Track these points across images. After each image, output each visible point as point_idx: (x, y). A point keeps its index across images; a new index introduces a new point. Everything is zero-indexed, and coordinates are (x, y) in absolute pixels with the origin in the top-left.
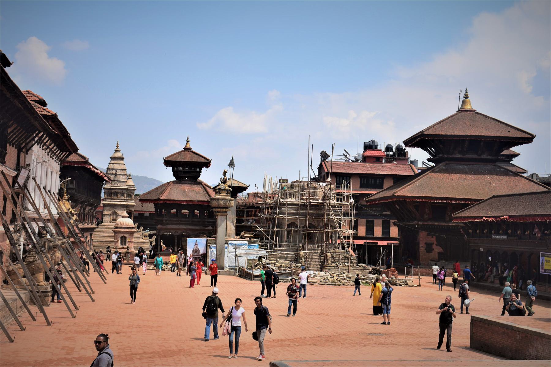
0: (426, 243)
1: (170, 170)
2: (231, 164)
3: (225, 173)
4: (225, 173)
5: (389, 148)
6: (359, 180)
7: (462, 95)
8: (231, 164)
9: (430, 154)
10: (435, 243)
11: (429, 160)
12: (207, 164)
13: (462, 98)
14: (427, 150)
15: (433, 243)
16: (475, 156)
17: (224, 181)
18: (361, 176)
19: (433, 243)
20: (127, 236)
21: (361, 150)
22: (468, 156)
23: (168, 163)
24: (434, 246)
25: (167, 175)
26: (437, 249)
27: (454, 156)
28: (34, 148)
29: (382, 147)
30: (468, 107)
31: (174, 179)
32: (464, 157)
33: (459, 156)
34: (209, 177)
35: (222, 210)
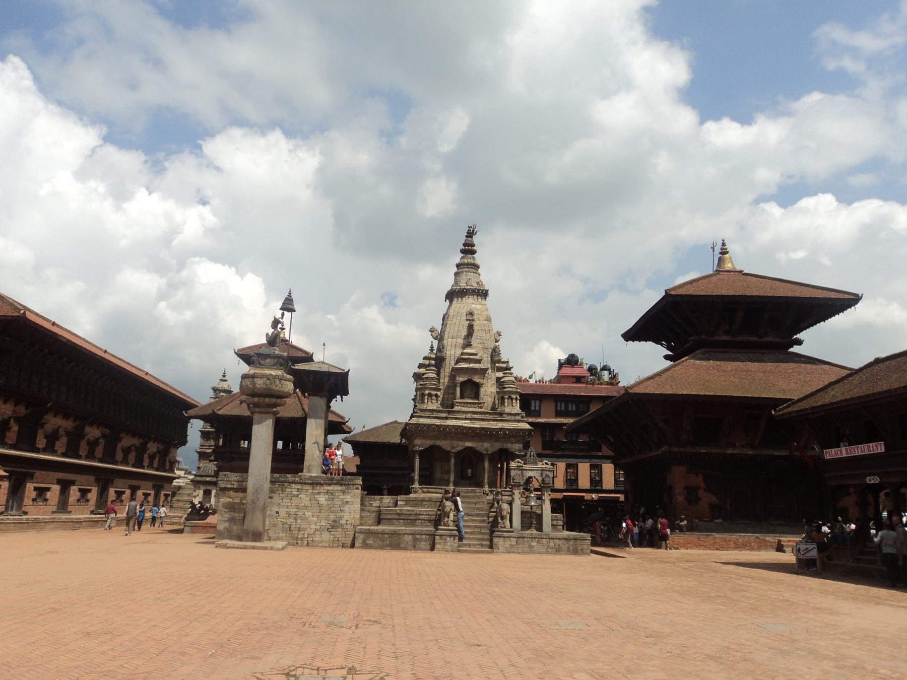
0: (686, 488)
4: (276, 323)
6: (553, 405)
7: (718, 249)
9: (669, 348)
10: (703, 486)
11: (667, 357)
15: (699, 488)
16: (755, 339)
17: (273, 340)
18: (557, 398)
19: (699, 488)
22: (739, 338)
24: (701, 493)
26: (707, 499)
27: (717, 338)
30: (728, 266)
32: (735, 339)
35: (261, 400)
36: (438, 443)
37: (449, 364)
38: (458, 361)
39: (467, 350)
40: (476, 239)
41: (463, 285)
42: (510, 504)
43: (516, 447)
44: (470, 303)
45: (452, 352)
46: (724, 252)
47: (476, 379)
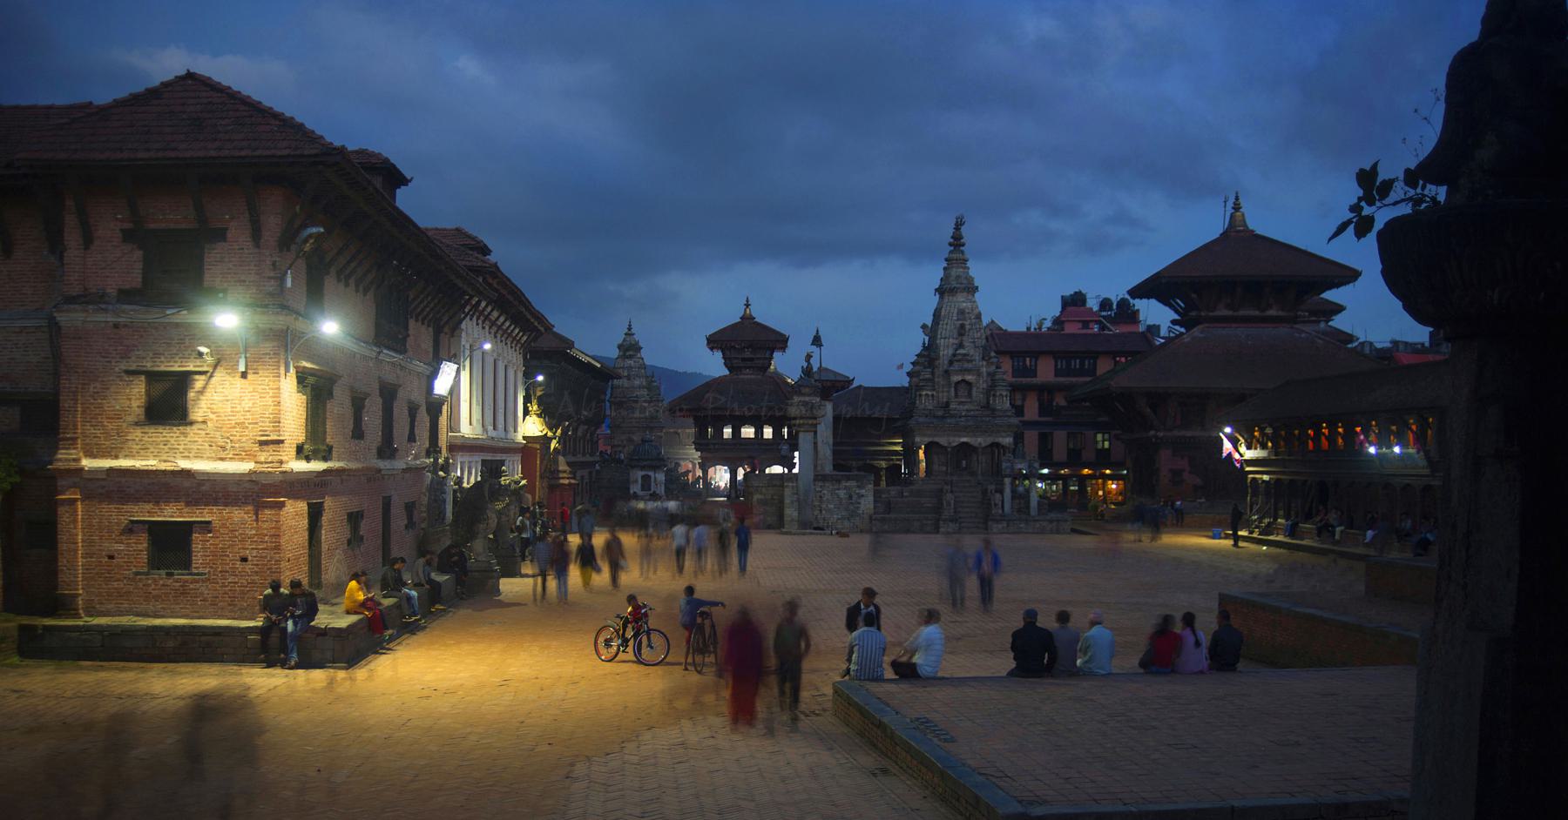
1: (719, 355)
2: (817, 341)
3: (809, 357)
4: (809, 357)
5: (1105, 304)
7: (1230, 204)
8: (817, 341)
9: (1176, 311)
12: (780, 342)
13: (1230, 211)
14: (1171, 306)
16: (1257, 313)
20: (651, 474)
21: (1056, 310)
22: (1242, 313)
23: (714, 342)
25: (714, 366)
27: (1217, 313)
28: (463, 326)
29: (1093, 304)
31: (727, 372)
33: (1230, 313)
34: (786, 365)
36: (936, 439)
37: (943, 362)
38: (951, 363)
39: (961, 351)
40: (963, 229)
41: (954, 284)
42: (1001, 492)
43: (1007, 441)
44: (961, 300)
45: (945, 352)
46: (1237, 207)
47: (969, 378)
